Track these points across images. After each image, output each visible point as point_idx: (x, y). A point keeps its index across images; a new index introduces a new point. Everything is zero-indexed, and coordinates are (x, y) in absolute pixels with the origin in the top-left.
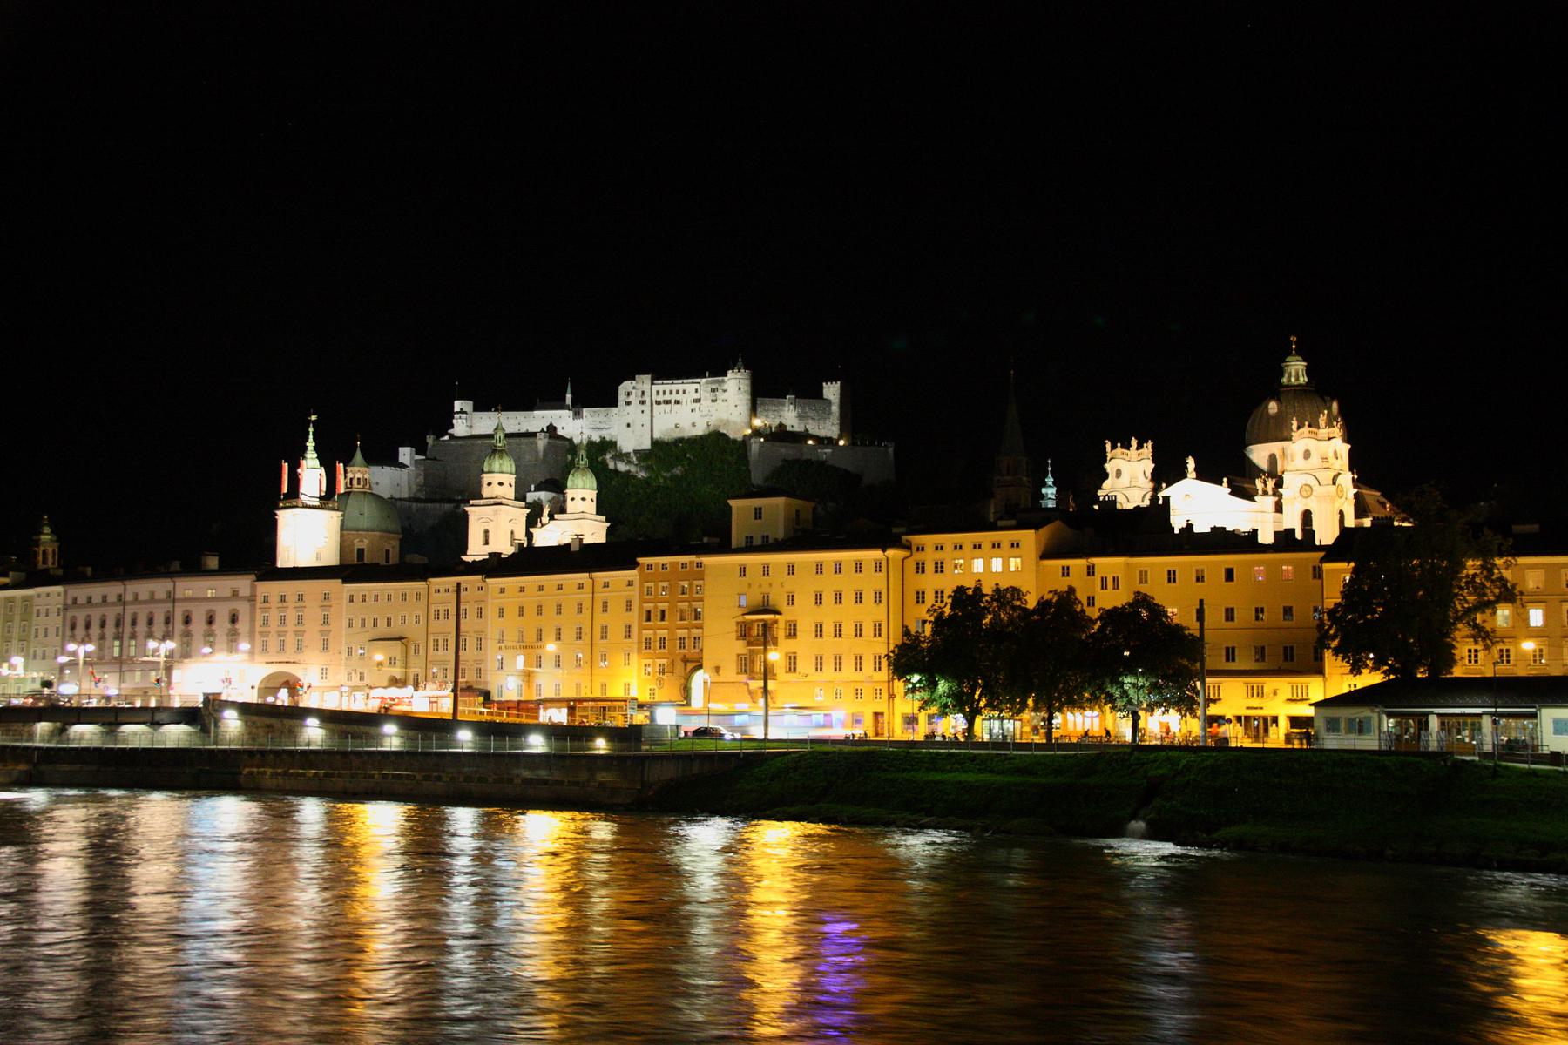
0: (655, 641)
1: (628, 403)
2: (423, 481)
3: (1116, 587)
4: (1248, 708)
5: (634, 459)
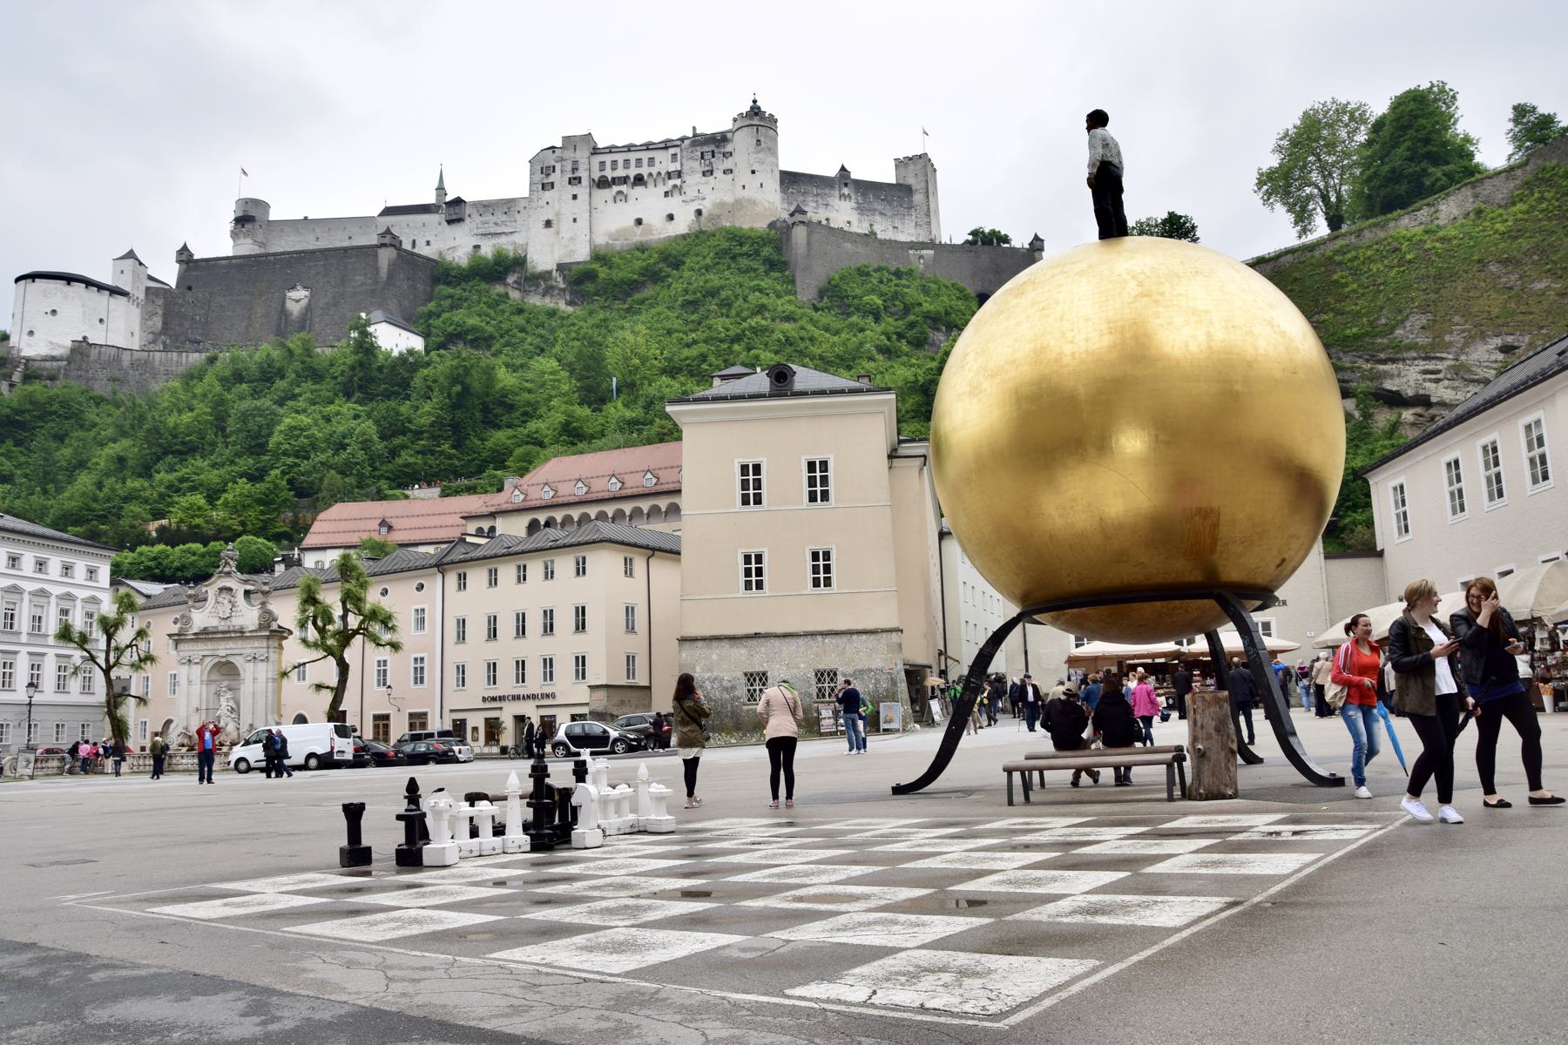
2: (160, 325)
5: (560, 279)
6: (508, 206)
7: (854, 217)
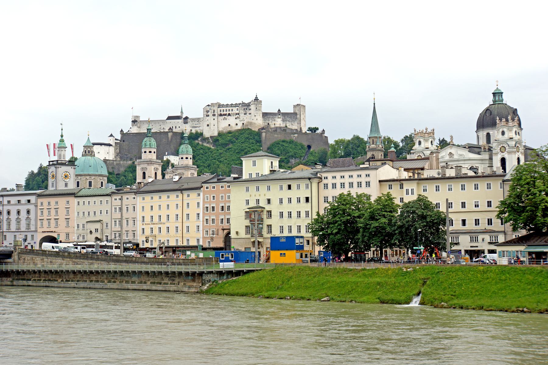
0: (210, 221)
1: (208, 116)
2: (118, 151)
3: (412, 193)
4: (471, 247)
6: (199, 119)
7: (281, 123)
